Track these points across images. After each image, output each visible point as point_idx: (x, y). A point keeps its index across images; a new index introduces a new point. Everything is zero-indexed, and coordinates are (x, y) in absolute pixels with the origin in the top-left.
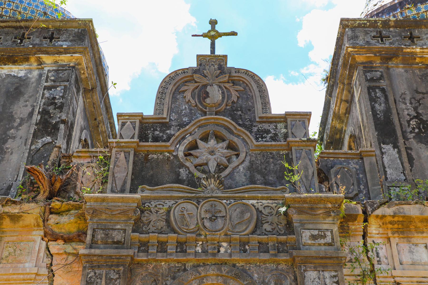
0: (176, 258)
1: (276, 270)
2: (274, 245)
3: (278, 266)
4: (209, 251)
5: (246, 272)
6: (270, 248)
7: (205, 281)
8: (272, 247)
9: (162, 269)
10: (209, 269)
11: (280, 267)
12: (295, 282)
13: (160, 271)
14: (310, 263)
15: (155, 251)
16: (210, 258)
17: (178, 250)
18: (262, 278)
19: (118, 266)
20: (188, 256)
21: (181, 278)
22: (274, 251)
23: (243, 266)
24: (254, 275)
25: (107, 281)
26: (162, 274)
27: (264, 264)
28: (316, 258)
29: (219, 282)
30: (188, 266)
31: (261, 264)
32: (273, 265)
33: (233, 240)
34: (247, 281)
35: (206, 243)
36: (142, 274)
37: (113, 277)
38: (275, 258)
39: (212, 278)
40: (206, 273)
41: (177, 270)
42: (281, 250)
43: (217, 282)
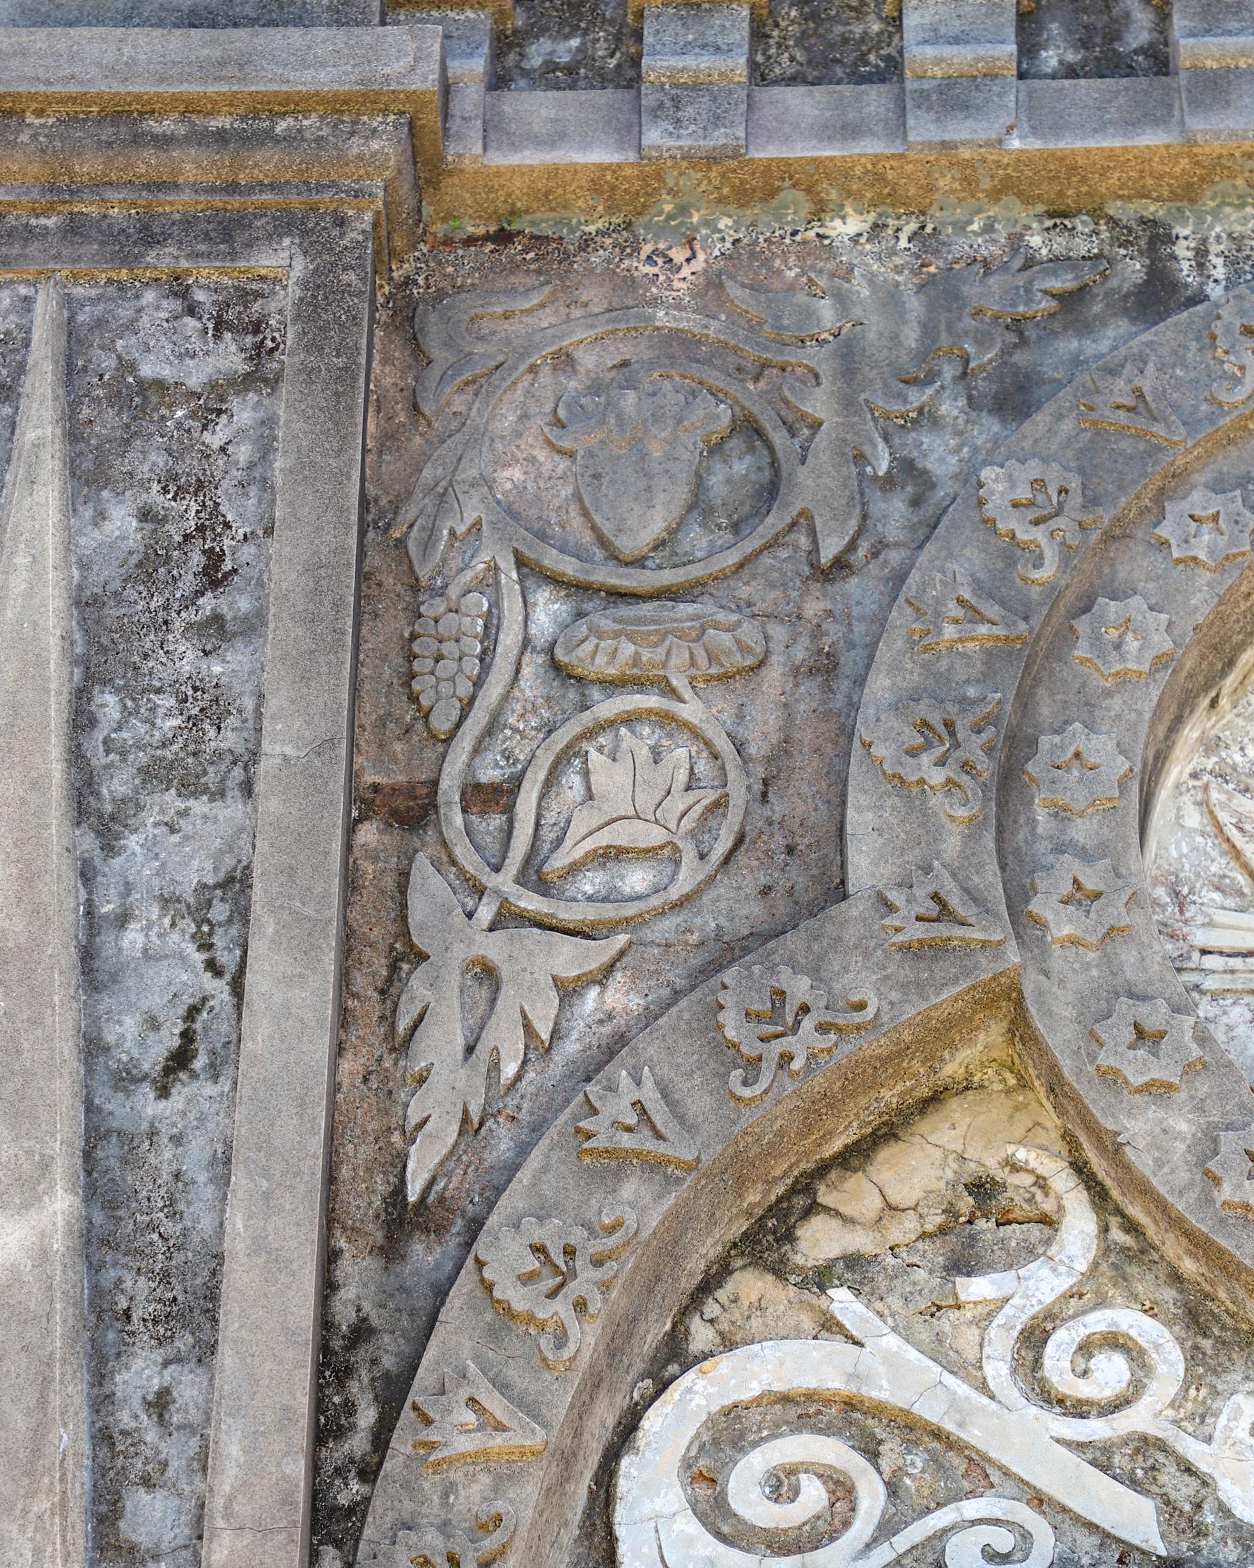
0: (1036, 144)
9: (842, 300)
13: (809, 314)
15: (738, 64)
17: (1050, 58)
19: (227, 238)
20: (1196, 104)
21: (1119, 389)
25: (86, 412)
30: (1201, 254)
37: (167, 373)
41: (1047, 304)
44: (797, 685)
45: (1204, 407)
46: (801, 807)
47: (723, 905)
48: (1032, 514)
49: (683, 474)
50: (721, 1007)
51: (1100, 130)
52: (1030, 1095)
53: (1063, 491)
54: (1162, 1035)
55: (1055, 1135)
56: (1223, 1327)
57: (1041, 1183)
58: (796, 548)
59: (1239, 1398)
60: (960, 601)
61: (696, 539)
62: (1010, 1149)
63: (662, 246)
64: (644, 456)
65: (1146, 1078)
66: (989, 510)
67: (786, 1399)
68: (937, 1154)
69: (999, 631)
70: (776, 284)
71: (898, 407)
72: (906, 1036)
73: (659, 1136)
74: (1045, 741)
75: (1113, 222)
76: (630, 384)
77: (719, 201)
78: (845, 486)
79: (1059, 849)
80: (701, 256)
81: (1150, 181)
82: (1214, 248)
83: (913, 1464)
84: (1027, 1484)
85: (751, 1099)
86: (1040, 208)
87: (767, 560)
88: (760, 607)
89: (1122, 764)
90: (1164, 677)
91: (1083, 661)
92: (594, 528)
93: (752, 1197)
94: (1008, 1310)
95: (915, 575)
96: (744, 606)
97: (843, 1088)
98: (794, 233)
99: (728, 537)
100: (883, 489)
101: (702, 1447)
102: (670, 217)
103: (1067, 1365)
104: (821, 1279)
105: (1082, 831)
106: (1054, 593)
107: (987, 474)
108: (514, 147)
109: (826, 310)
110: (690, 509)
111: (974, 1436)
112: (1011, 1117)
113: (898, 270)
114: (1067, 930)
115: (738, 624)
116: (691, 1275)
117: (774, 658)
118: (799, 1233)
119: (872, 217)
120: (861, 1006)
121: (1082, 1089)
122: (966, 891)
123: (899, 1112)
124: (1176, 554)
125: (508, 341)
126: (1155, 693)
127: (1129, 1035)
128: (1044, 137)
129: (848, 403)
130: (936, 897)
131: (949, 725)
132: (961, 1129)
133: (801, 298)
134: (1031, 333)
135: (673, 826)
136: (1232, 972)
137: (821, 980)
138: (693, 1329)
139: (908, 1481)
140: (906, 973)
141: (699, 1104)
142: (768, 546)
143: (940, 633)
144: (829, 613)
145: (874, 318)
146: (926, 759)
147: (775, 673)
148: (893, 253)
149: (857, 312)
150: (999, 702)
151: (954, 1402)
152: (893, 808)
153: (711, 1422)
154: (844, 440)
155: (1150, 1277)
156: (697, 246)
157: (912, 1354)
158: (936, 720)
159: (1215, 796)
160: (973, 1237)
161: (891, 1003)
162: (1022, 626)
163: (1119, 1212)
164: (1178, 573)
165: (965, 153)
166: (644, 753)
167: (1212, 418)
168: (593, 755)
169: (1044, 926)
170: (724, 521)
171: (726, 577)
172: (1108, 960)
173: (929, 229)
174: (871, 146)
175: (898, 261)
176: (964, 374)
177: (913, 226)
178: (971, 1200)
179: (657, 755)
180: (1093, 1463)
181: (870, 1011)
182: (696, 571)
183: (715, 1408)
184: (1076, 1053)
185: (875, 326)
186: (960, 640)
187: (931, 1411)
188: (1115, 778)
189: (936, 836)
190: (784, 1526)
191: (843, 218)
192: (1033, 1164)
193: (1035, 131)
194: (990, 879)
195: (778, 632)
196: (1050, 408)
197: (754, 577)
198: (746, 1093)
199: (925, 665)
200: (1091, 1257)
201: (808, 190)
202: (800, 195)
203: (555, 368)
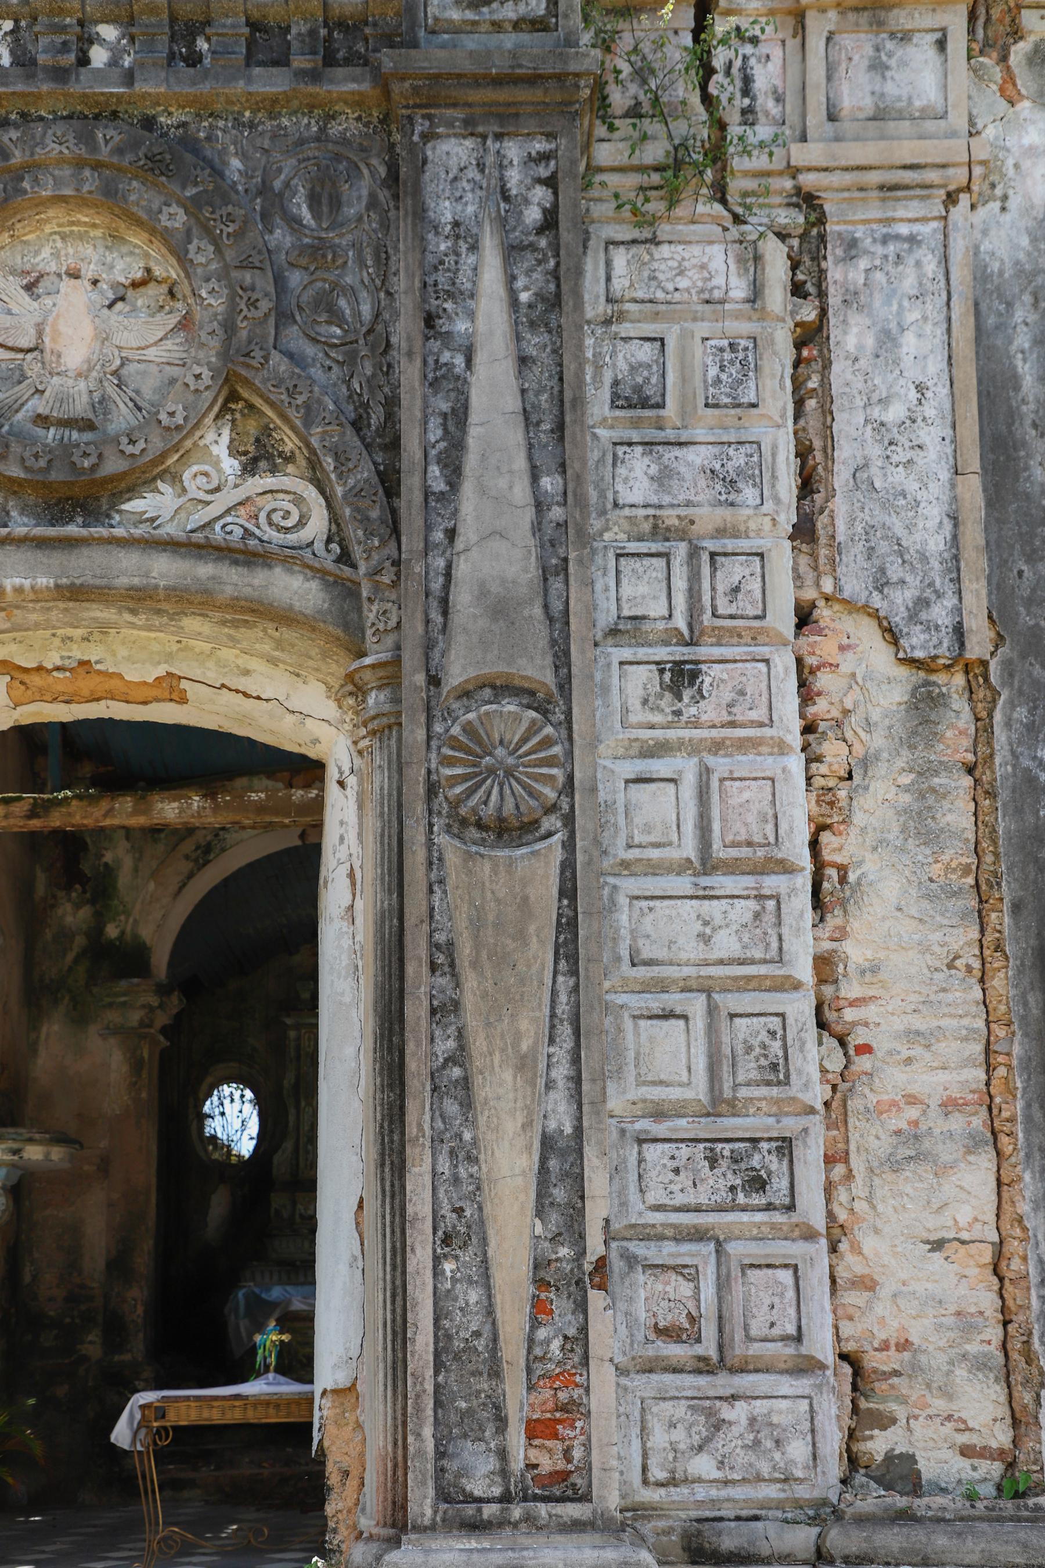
1: (318, 139)
2: (313, 33)
3: (325, 125)
4: (42, 59)
5: (196, 151)
6: (295, 46)
7: (26, 185)
8: (303, 41)
10: (45, 134)
11: (335, 129)
12: (389, 187)
14: (448, 106)
16: (45, 88)
18: (259, 173)
22: (308, 57)
23: (184, 125)
24: (226, 164)
27: (273, 116)
28: (477, 81)
29: (86, 188)
31: (260, 115)
32: (306, 121)
33: (141, 13)
34: (196, 184)
35: (30, 26)
38: (311, 89)
39: (56, 172)
40: (32, 154)
42: (341, 55)
43: (77, 190)
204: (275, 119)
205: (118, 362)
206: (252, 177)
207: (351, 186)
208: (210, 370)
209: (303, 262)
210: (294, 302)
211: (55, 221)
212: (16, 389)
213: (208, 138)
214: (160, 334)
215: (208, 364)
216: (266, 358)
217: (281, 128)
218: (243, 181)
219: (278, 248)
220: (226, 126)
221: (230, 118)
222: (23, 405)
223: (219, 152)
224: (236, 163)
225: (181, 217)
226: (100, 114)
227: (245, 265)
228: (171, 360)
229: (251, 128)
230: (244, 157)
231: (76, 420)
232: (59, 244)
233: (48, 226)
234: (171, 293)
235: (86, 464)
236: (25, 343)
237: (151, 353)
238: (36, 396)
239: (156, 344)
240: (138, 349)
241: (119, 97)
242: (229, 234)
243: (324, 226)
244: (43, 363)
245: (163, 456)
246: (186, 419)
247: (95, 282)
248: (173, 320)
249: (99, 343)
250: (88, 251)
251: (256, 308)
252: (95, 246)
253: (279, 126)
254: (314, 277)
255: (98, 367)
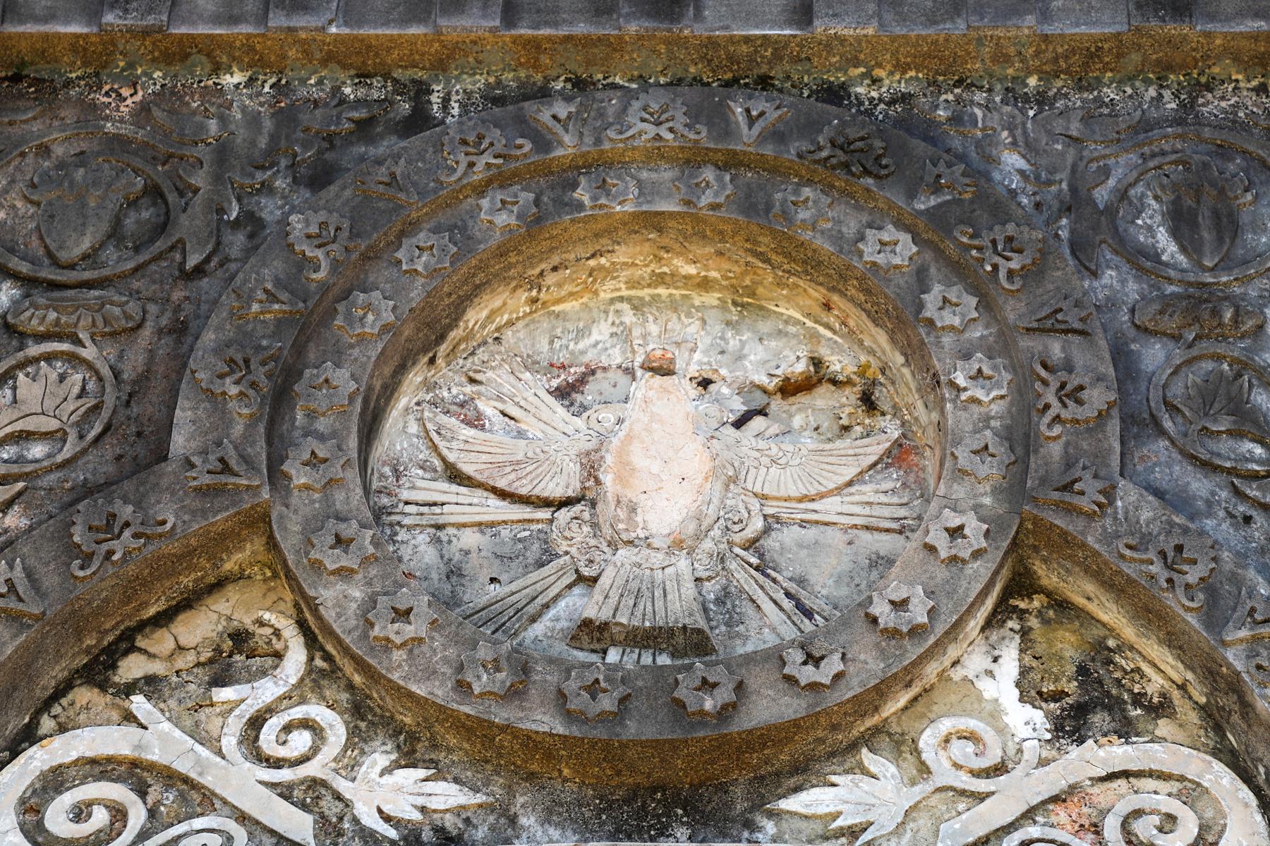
1: (1179, 121)
3: (1193, 101)
9: (223, 120)
11: (1212, 106)
13: (202, 128)
18: (1063, 175)
26: (223, 151)
30: (446, 101)
32: (1152, 92)
36: (44, 150)
41: (347, 125)
44: (160, 339)
45: (432, 184)
46: (150, 409)
47: (91, 466)
48: (316, 242)
49: (107, 216)
50: (74, 523)
51: (386, 24)
52: (279, 581)
53: (338, 229)
54: (352, 540)
55: (290, 604)
56: (375, 715)
57: (277, 633)
58: (173, 260)
59: (376, 755)
60: (266, 291)
61: (110, 254)
62: (260, 613)
63: (116, 86)
64: (84, 206)
65: (337, 566)
66: (291, 238)
67: (93, 762)
68: (215, 616)
69: (284, 307)
70: (185, 110)
71: (248, 181)
72: (193, 542)
73: (20, 600)
74: (307, 373)
75: (395, 81)
76: (83, 164)
77: (154, 60)
78: (208, 225)
79: (305, 435)
80: (140, 93)
81: (417, 57)
82: (454, 98)
83: (167, 798)
84: (236, 808)
85: (84, 578)
86: (353, 72)
87: (153, 267)
88: (144, 294)
89: (353, 386)
90: (387, 337)
91: (340, 328)
92: (46, 247)
93: (90, 642)
94: (243, 706)
95: (241, 275)
96: (135, 294)
97: (150, 574)
98: (200, 81)
99: (131, 253)
100: (232, 228)
101: (34, 792)
102: (123, 70)
103: (274, 738)
104: (129, 689)
105: (322, 425)
106: (325, 287)
107: (293, 218)
108: (22, 21)
109: (213, 125)
110: (109, 237)
111: (207, 781)
112: (265, 595)
113: (261, 104)
114: (303, 481)
115: (127, 302)
116: (44, 688)
117: (148, 323)
118: (119, 664)
119: (249, 73)
120: (164, 522)
121: (298, 573)
122: (241, 456)
123: (194, 592)
124: (404, 267)
125: (9, 138)
126: (380, 346)
127: (331, 540)
128: (351, 27)
129: (218, 179)
130: (222, 460)
131: (247, 361)
132: (232, 602)
133: (198, 118)
134: (338, 142)
135: (65, 419)
136: (422, 514)
137: (141, 508)
138: (42, 722)
139: (162, 808)
140: (197, 504)
141: (50, 581)
142: (155, 259)
143: (250, 307)
144: (187, 298)
145: (242, 131)
146: (228, 380)
147: (147, 332)
148: (259, 94)
149: (232, 127)
150: (280, 348)
151: (199, 761)
152: (205, 409)
153: (43, 776)
154: (212, 200)
155: (334, 686)
156: (139, 87)
157: (178, 733)
158: (239, 358)
159: (426, 414)
160: (229, 665)
161: (184, 522)
162: (301, 305)
163: (322, 649)
164: (405, 279)
165: (303, 35)
166: (54, 376)
167: (435, 191)
168: (21, 376)
169: (290, 479)
170: (130, 245)
171: (126, 276)
172: (327, 500)
173: (283, 82)
174: (245, 29)
175: (262, 99)
176: (293, 164)
177: (274, 80)
178: (230, 643)
179: (62, 378)
180: (281, 795)
181: (168, 526)
182: (106, 272)
183: (46, 768)
184: (298, 552)
185: (242, 135)
186: (262, 313)
187: (182, 767)
188: (346, 394)
189: (229, 424)
190: (77, 836)
191: (232, 74)
192: (273, 622)
193: (346, 24)
194: (259, 450)
195: (153, 309)
196: (339, 182)
197: (143, 276)
198: (81, 574)
199: (239, 327)
200: (299, 675)
201: (208, 55)
202: (204, 59)
203: (37, 154)
204: (1090, 89)
205: (759, 524)
206: (1049, 183)
207: (1256, 197)
208: (982, 519)
209: (1171, 324)
210: (1155, 396)
211: (625, 274)
212: (534, 576)
213: (955, 120)
214: (849, 473)
215: (977, 508)
216: (1109, 493)
217: (1103, 104)
218: (1030, 189)
219: (1112, 304)
220: (988, 101)
221: (998, 87)
222: (546, 606)
223: (978, 144)
224: (1013, 160)
225: (905, 248)
226: (735, 81)
227: (1050, 326)
228: (874, 522)
229: (1040, 103)
230: (1029, 148)
231: (671, 632)
232: (629, 317)
233: (610, 284)
234: (868, 402)
235: (709, 705)
236: (554, 488)
237: (830, 508)
238: (577, 590)
239: (838, 490)
240: (800, 500)
241: (779, 46)
242: (1011, 274)
243: (1208, 263)
244: (595, 526)
245: (881, 691)
246: (932, 612)
247: (705, 383)
248: (875, 449)
249: (719, 486)
250: (693, 329)
251: (1080, 402)
252: (704, 322)
253: (1099, 102)
254: (1195, 352)
255: (716, 532)
